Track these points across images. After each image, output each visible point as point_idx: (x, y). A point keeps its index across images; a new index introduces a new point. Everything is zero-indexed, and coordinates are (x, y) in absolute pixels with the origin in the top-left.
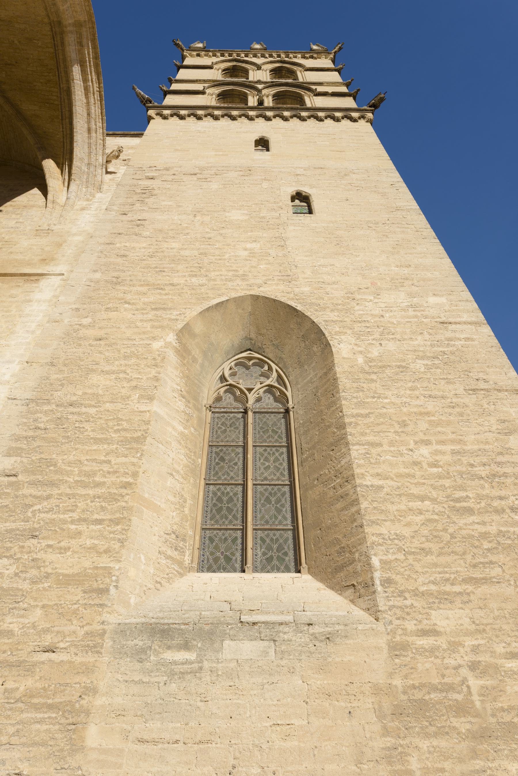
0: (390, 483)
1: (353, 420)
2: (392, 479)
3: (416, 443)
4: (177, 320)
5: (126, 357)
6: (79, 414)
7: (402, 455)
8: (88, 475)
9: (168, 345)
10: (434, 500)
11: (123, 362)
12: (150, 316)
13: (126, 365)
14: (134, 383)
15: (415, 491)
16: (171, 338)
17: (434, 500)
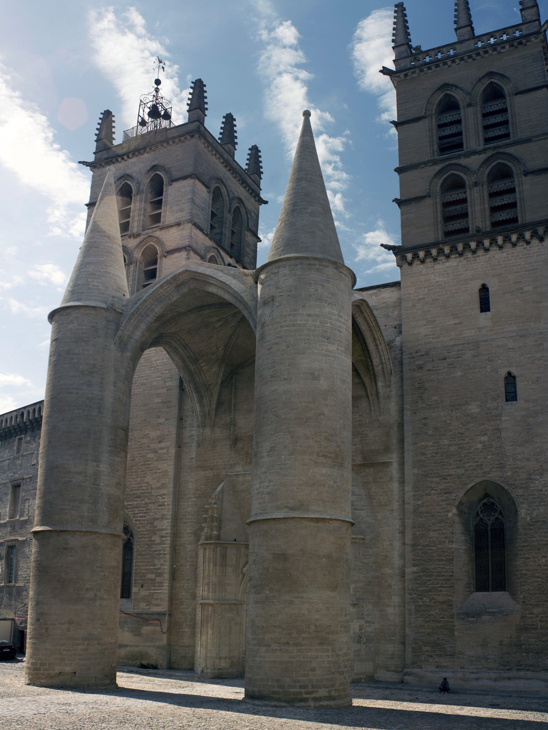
0: (530, 572)
1: (522, 548)
2: (531, 571)
3: (542, 557)
4: (455, 499)
5: (440, 522)
6: (430, 550)
7: (536, 562)
8: (440, 572)
9: (454, 514)
10: (542, 578)
11: (440, 525)
12: (444, 498)
13: (441, 527)
14: (445, 536)
15: (537, 575)
16: (455, 511)
17: (542, 578)
